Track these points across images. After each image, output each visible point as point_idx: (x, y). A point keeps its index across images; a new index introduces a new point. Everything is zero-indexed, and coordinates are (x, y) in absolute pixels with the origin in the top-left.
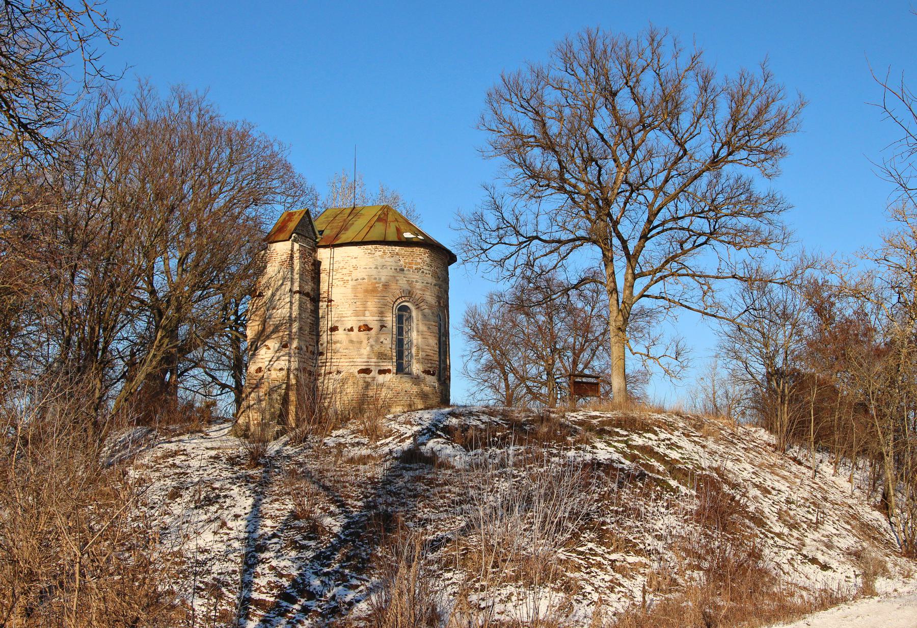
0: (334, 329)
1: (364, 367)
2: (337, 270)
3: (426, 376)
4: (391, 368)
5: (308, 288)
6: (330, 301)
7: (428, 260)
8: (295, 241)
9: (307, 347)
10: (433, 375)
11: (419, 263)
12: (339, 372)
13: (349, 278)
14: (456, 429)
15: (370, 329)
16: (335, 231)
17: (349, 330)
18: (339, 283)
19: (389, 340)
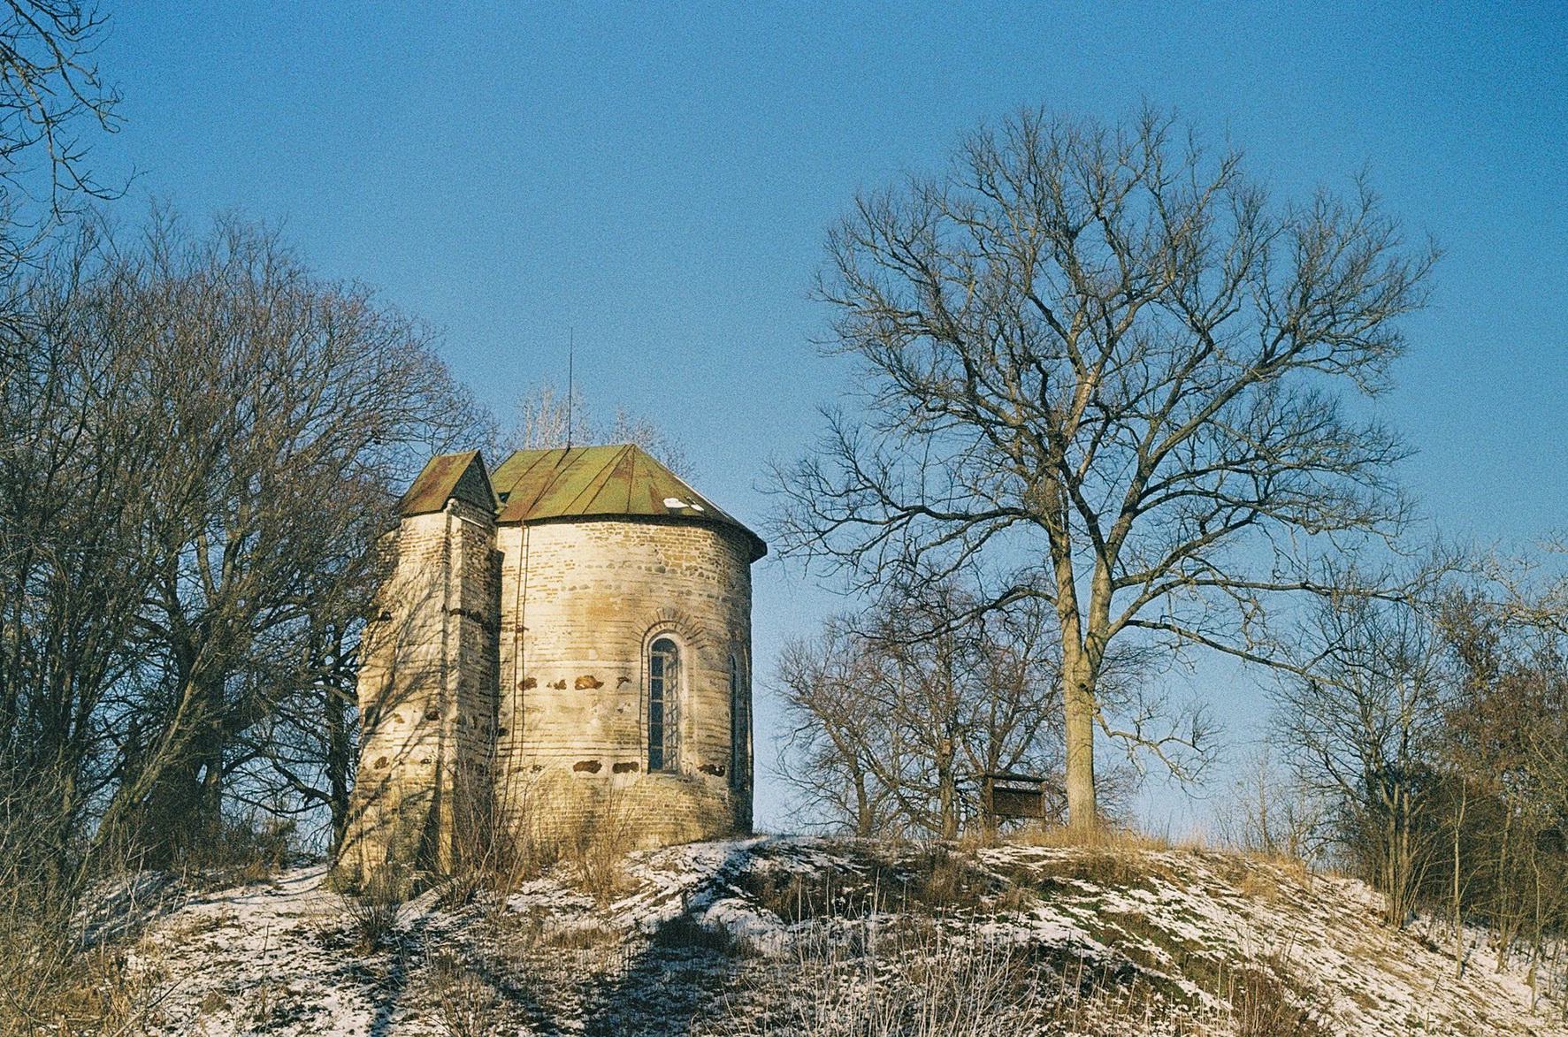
0: (528, 684)
1: (587, 759)
3: (707, 777)
4: (638, 760)
5: (478, 605)
6: (521, 630)
7: (711, 552)
8: (453, 512)
10: (720, 774)
11: (693, 558)
12: (536, 768)
13: (558, 586)
14: (764, 880)
15: (598, 685)
16: (532, 494)
17: (557, 687)
18: (537, 595)
19: (635, 704)
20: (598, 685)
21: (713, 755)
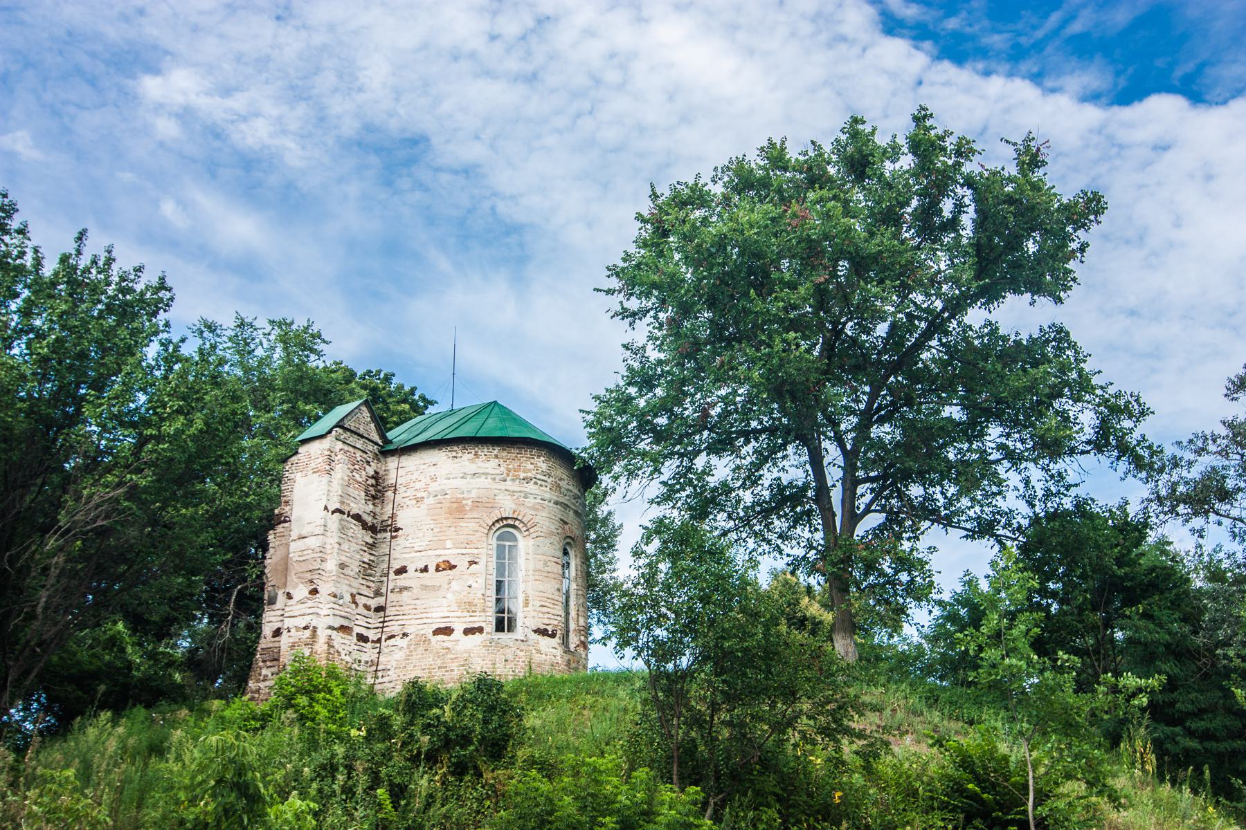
0: (402, 571)
1: (443, 626)
2: (407, 486)
3: (539, 637)
4: (483, 624)
6: (397, 530)
7: (544, 467)
9: (353, 596)
10: (553, 635)
11: (530, 471)
12: (405, 635)
13: (425, 494)
15: (453, 567)
17: (422, 571)
19: (481, 581)
20: (453, 567)
21: (547, 621)
